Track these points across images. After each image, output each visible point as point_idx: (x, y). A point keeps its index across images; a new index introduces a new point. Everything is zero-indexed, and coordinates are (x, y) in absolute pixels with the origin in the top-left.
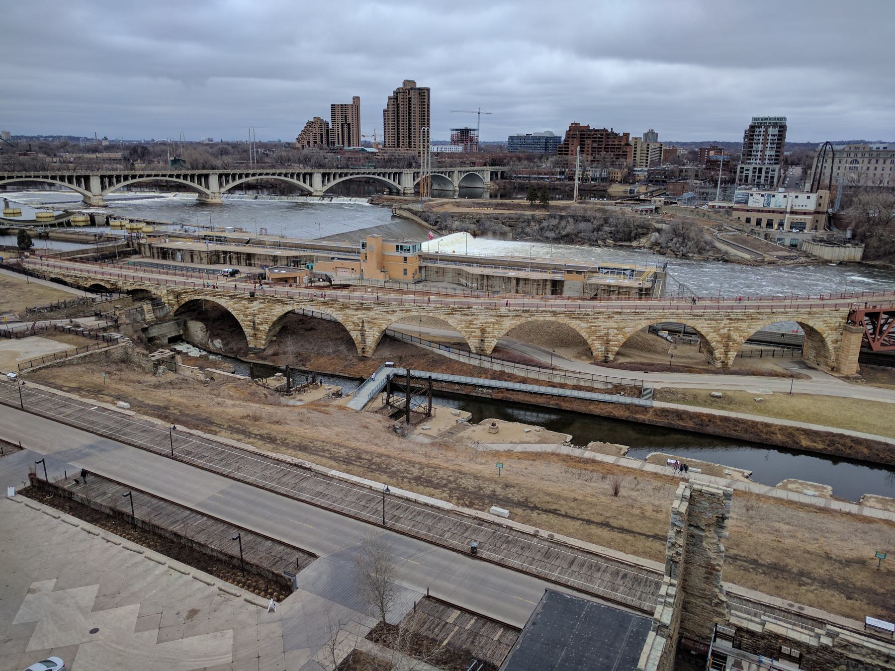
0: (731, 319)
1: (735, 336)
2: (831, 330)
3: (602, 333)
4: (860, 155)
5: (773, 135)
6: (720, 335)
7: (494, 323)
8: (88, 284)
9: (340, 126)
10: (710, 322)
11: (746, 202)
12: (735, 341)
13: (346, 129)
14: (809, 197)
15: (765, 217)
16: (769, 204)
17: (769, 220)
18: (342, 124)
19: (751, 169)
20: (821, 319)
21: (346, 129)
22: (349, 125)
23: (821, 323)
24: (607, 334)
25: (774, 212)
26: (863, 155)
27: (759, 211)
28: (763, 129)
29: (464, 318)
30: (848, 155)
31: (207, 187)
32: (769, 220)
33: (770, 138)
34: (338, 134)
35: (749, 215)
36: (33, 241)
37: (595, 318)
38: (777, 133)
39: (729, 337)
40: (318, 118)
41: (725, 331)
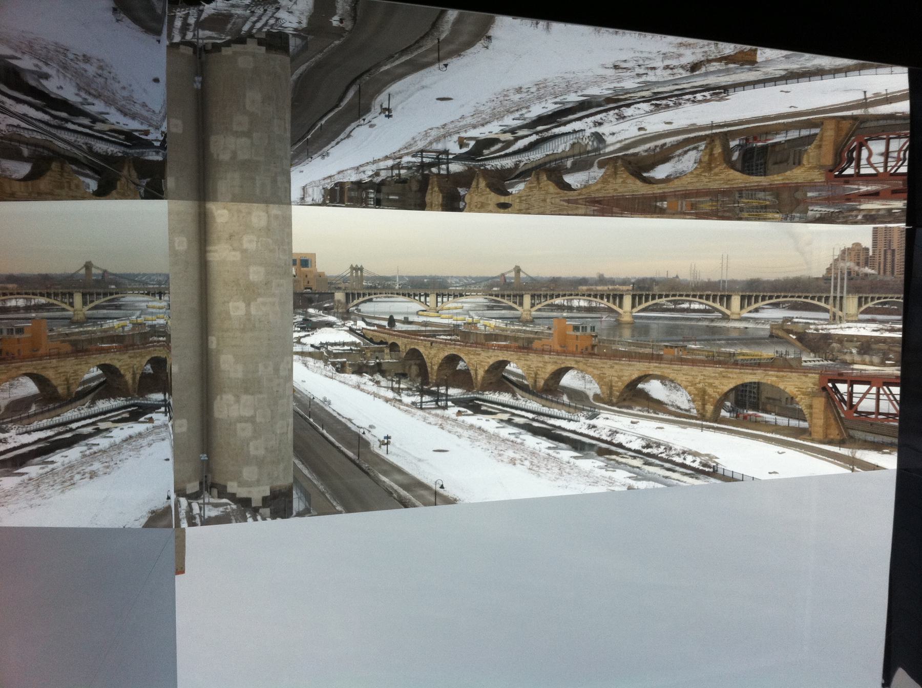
0: (704, 375)
1: (710, 391)
2: (804, 394)
3: (607, 380)
6: (696, 389)
7: (542, 368)
8: (379, 341)
9: (882, 253)
10: (687, 377)
12: (710, 396)
13: (889, 257)
18: (885, 251)
20: (791, 383)
21: (889, 257)
22: (894, 251)
23: (793, 387)
24: (611, 381)
29: (526, 362)
31: (621, 306)
34: (880, 264)
36: (396, 324)
37: (602, 367)
39: (704, 392)
40: (858, 244)
41: (700, 386)
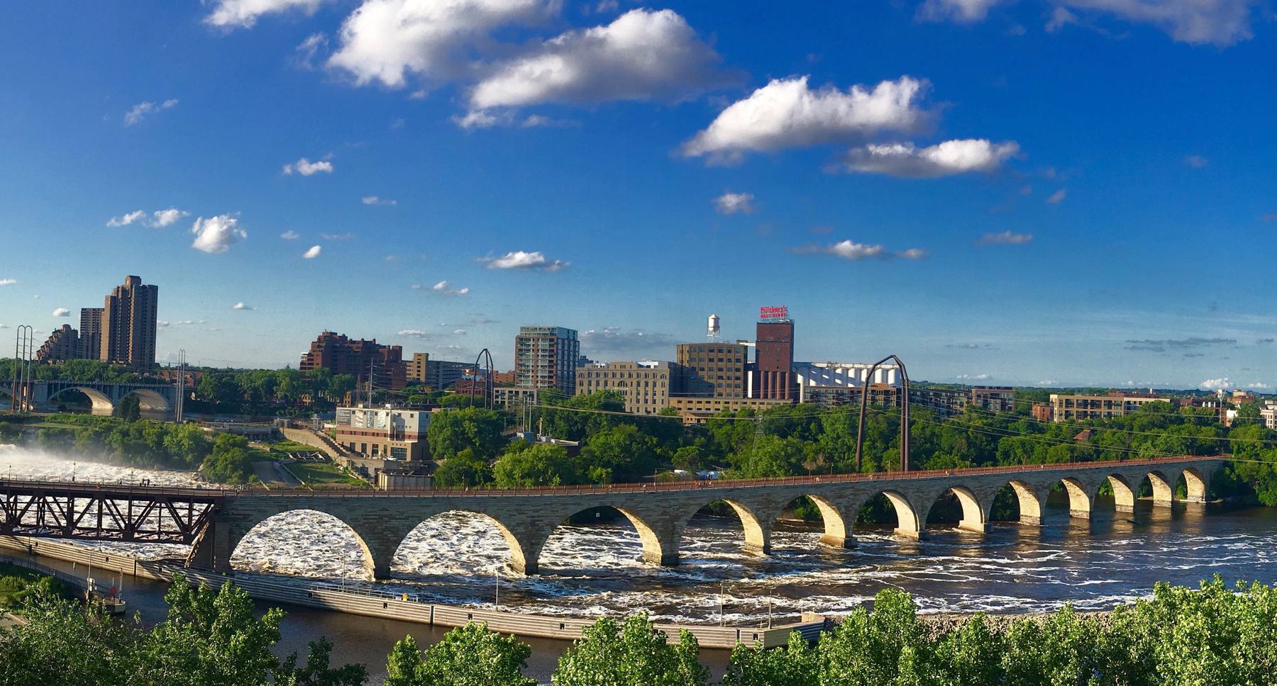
4: (626, 376)
5: (543, 350)
11: (349, 423)
14: (412, 416)
15: (370, 441)
16: (372, 425)
17: (363, 444)
19: (507, 392)
25: (378, 435)
26: (630, 376)
27: (363, 434)
28: (531, 343)
30: (614, 375)
32: (363, 444)
33: (540, 353)
35: (352, 439)
38: (548, 348)
